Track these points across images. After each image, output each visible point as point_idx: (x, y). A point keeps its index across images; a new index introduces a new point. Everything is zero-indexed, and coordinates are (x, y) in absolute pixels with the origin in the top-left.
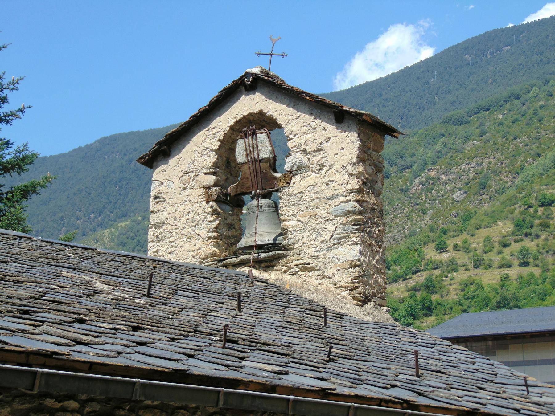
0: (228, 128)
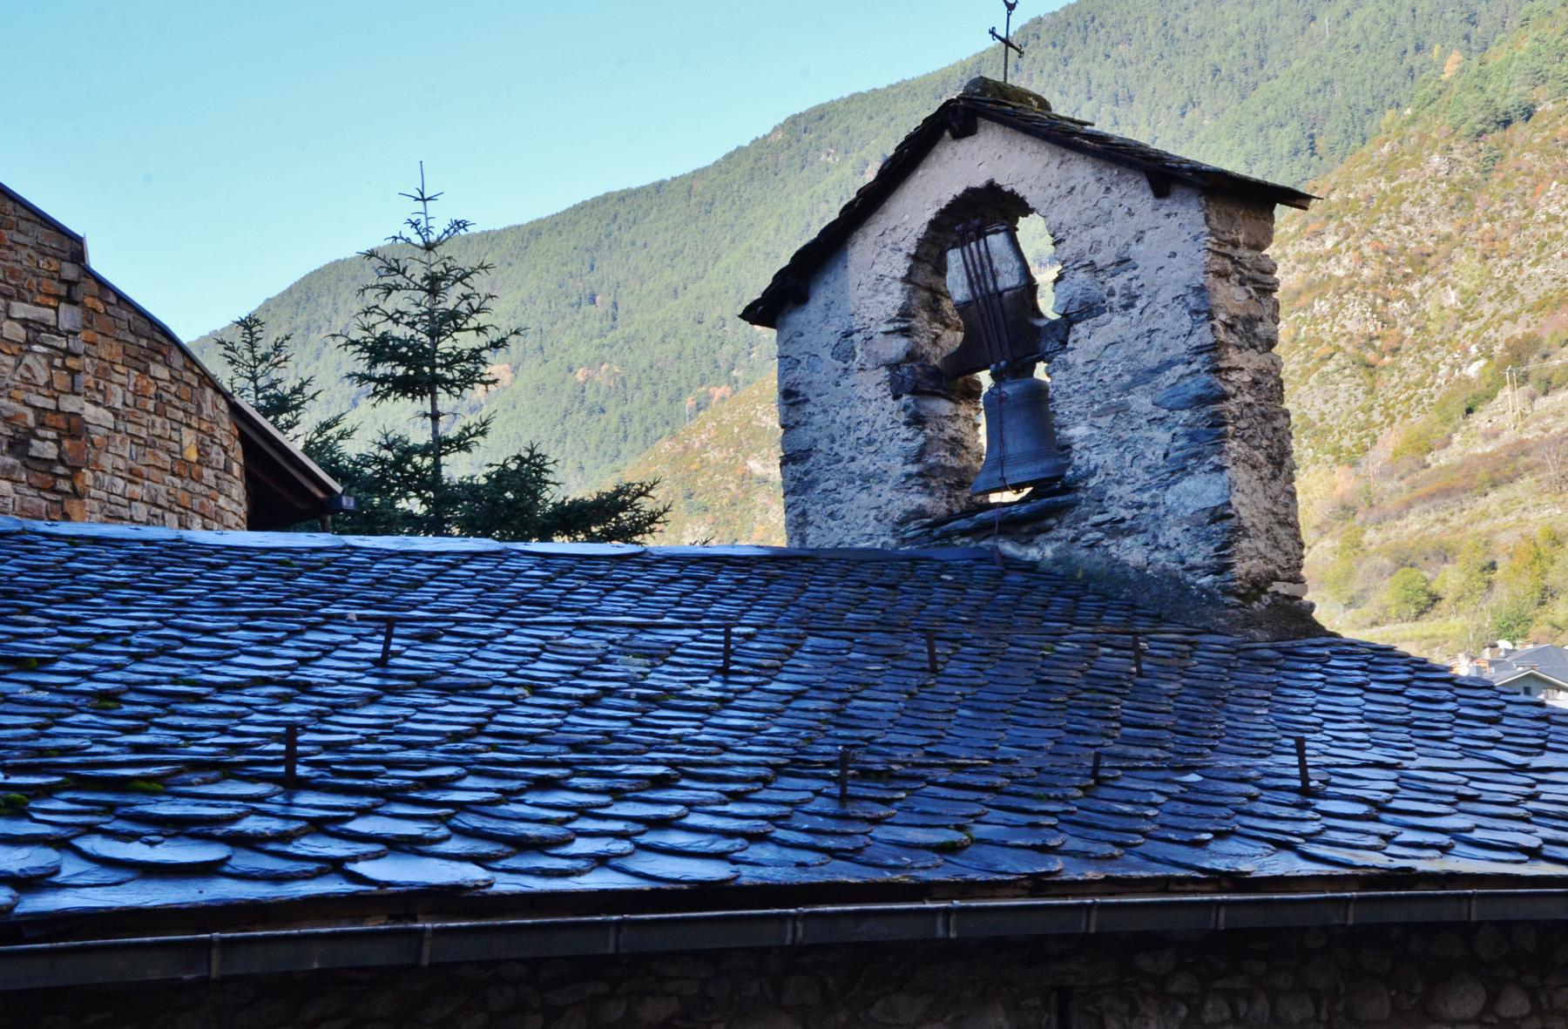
0: (925, 227)
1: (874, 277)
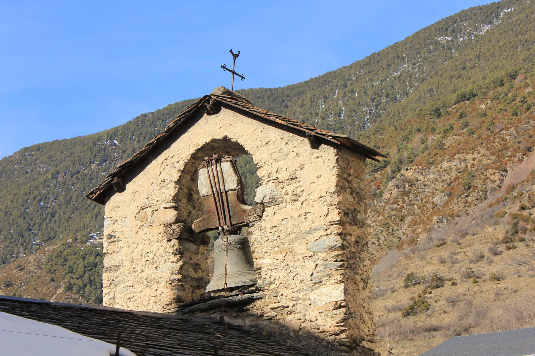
0: (189, 157)
1: (161, 180)
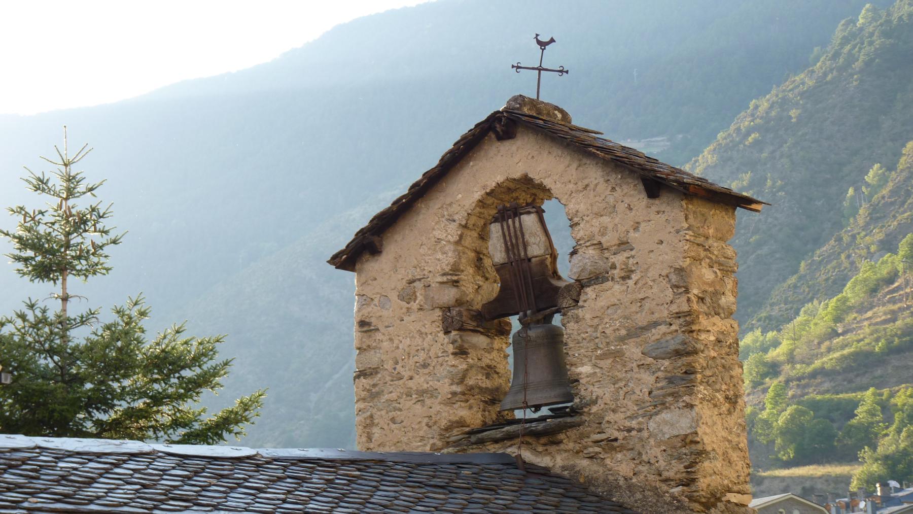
1: (433, 240)
